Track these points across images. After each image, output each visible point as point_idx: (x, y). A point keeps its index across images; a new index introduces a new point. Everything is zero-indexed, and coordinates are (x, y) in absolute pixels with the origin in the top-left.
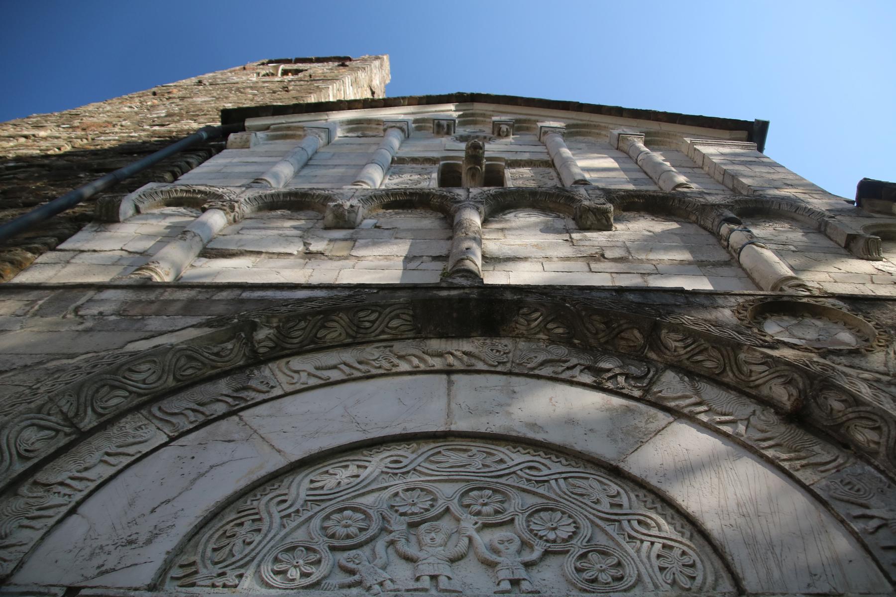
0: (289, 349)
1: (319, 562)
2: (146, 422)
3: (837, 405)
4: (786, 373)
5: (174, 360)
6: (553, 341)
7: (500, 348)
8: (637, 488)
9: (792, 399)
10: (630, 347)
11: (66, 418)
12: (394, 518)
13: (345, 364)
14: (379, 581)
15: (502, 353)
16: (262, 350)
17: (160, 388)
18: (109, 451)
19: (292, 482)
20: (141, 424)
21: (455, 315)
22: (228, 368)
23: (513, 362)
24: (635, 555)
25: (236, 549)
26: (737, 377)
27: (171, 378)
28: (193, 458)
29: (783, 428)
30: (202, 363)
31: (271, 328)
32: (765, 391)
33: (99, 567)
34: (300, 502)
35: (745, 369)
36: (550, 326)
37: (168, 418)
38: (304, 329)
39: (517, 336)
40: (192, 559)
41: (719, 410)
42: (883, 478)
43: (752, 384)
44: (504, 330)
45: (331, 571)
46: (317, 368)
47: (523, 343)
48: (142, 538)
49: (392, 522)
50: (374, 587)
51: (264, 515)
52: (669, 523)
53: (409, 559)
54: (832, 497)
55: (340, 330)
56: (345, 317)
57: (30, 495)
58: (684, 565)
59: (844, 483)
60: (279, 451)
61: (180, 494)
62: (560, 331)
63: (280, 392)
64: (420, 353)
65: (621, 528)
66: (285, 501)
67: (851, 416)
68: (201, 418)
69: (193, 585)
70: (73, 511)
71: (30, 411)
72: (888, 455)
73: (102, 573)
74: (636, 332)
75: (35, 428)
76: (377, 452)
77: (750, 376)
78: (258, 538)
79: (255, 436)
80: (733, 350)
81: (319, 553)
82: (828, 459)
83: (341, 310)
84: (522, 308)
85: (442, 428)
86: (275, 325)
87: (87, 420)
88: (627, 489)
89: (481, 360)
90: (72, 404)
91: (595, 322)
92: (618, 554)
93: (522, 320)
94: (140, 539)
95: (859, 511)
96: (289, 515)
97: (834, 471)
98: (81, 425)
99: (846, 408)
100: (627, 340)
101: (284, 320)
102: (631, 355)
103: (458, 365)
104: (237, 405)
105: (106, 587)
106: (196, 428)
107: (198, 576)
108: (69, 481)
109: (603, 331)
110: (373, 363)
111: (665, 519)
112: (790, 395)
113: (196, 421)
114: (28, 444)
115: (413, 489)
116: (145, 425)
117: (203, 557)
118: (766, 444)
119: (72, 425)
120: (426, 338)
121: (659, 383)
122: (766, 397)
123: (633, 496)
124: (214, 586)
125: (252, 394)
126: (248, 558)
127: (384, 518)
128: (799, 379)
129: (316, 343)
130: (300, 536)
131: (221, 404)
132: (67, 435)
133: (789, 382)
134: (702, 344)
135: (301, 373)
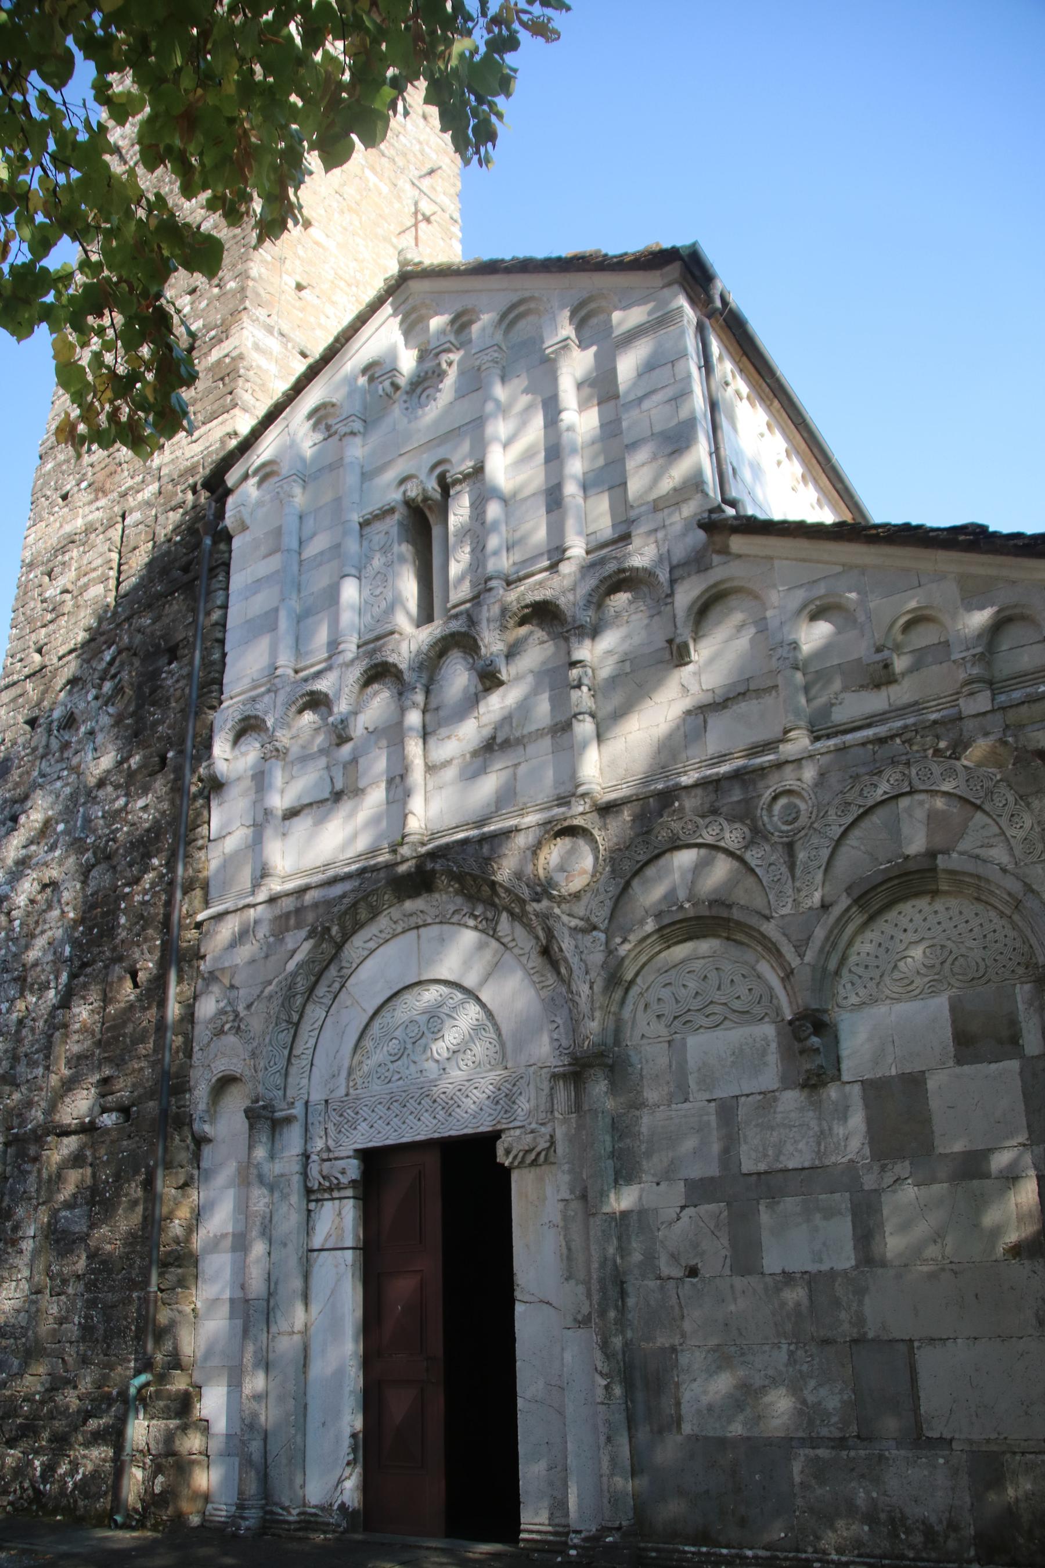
7: (435, 903)
11: (287, 1022)
16: (339, 940)
70: (312, 1065)
103: (421, 923)
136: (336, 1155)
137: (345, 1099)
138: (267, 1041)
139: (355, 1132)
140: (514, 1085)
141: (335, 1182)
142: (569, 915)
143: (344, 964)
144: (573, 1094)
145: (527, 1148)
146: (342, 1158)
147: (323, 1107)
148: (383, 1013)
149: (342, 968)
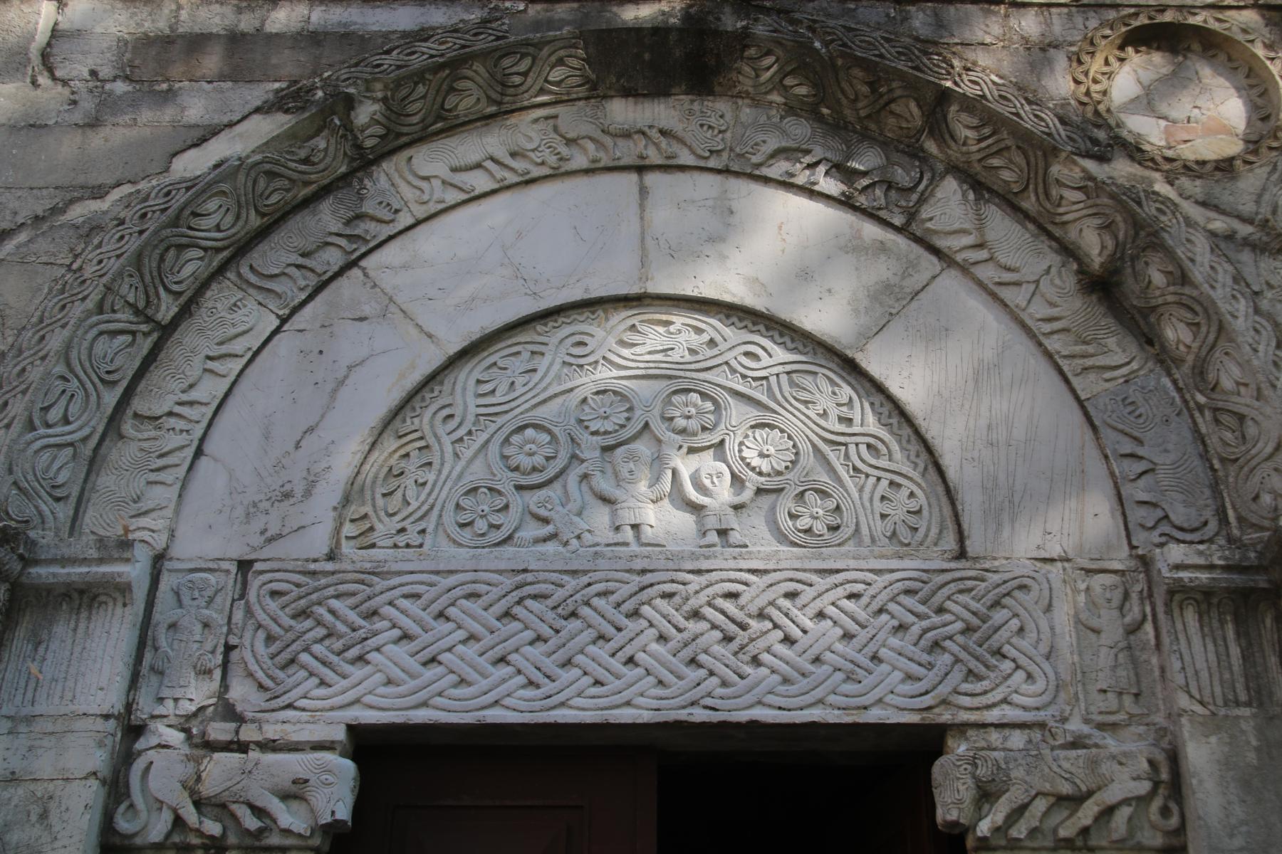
0: (407, 134)
1: (506, 507)
2: (240, 295)
3: (1158, 279)
4: (1107, 212)
5: (250, 184)
6: (791, 109)
7: (713, 121)
8: (873, 390)
9: (1106, 253)
10: (901, 128)
11: (137, 312)
12: (585, 438)
13: (493, 159)
14: (576, 534)
15: (716, 131)
16: (369, 143)
17: (243, 233)
18: (211, 354)
19: (454, 383)
20: (235, 299)
21: (647, 56)
22: (326, 182)
23: (731, 150)
24: (856, 495)
25: (411, 494)
26: (1040, 204)
27: (253, 212)
28: (321, 352)
29: (1078, 303)
30: (290, 179)
31: (375, 100)
32: (1072, 234)
33: (262, 533)
34: (470, 418)
35: (1054, 192)
36: (789, 81)
37: (269, 285)
38: (424, 97)
39: (739, 96)
40: (363, 510)
41: (1003, 261)
42: (1178, 400)
43: (1058, 219)
44: (720, 84)
45: (521, 520)
46: (455, 170)
47: (748, 110)
48: (299, 490)
49: (583, 446)
50: (571, 541)
51: (431, 440)
52: (902, 449)
53: (606, 500)
54: (1105, 422)
55: (477, 93)
56: (482, 70)
58: (908, 512)
59: (1127, 402)
60: (430, 336)
61: (323, 416)
62: (803, 90)
63: (410, 221)
64: (597, 134)
65: (847, 456)
66: (451, 416)
67: (1170, 298)
68: (313, 281)
69: (373, 546)
70: (199, 453)
71: (89, 314)
72: (1194, 367)
73: (270, 540)
74: (913, 105)
75: (106, 336)
76: (554, 327)
77: (1059, 205)
78: (431, 477)
79: (392, 308)
80: (1045, 155)
81: (505, 496)
82: (1122, 362)
83: (472, 57)
84: (746, 47)
85: (635, 289)
86: (380, 95)
87: (163, 307)
88: (862, 392)
89: (685, 144)
90: (136, 288)
91: (855, 81)
92: (837, 493)
93: (747, 69)
94: (296, 490)
95: (1128, 447)
96: (461, 440)
97: (1122, 380)
98: (159, 317)
99: (1168, 286)
100: (898, 116)
101: (392, 86)
102: (902, 142)
103: (654, 157)
104: (355, 250)
105: (280, 559)
106: (310, 298)
107: (376, 534)
108: (178, 409)
109: (866, 97)
110: (531, 154)
111: (899, 442)
112: (1103, 247)
113: (307, 286)
114: (106, 363)
115: (604, 392)
116: (240, 300)
117: (374, 506)
118: (1047, 328)
119: (149, 320)
120: (605, 97)
121: (932, 201)
122: (1073, 243)
123: (867, 405)
124: (396, 546)
125: (372, 226)
126: (425, 508)
127: (572, 440)
128: (1122, 225)
129: (445, 119)
130: (477, 473)
131: (332, 249)
132: (146, 335)
133: (1108, 227)
134: (1004, 139)
135: (432, 180)
136: (271, 732)
137: (329, 566)
138: (55, 342)
139: (357, 672)
140: (996, 604)
141: (251, 823)
142: (1204, 204)
143: (369, 207)
144: (1235, 651)
145: (1066, 789)
146: (294, 748)
147: (229, 582)
148: (495, 355)
149: (360, 217)
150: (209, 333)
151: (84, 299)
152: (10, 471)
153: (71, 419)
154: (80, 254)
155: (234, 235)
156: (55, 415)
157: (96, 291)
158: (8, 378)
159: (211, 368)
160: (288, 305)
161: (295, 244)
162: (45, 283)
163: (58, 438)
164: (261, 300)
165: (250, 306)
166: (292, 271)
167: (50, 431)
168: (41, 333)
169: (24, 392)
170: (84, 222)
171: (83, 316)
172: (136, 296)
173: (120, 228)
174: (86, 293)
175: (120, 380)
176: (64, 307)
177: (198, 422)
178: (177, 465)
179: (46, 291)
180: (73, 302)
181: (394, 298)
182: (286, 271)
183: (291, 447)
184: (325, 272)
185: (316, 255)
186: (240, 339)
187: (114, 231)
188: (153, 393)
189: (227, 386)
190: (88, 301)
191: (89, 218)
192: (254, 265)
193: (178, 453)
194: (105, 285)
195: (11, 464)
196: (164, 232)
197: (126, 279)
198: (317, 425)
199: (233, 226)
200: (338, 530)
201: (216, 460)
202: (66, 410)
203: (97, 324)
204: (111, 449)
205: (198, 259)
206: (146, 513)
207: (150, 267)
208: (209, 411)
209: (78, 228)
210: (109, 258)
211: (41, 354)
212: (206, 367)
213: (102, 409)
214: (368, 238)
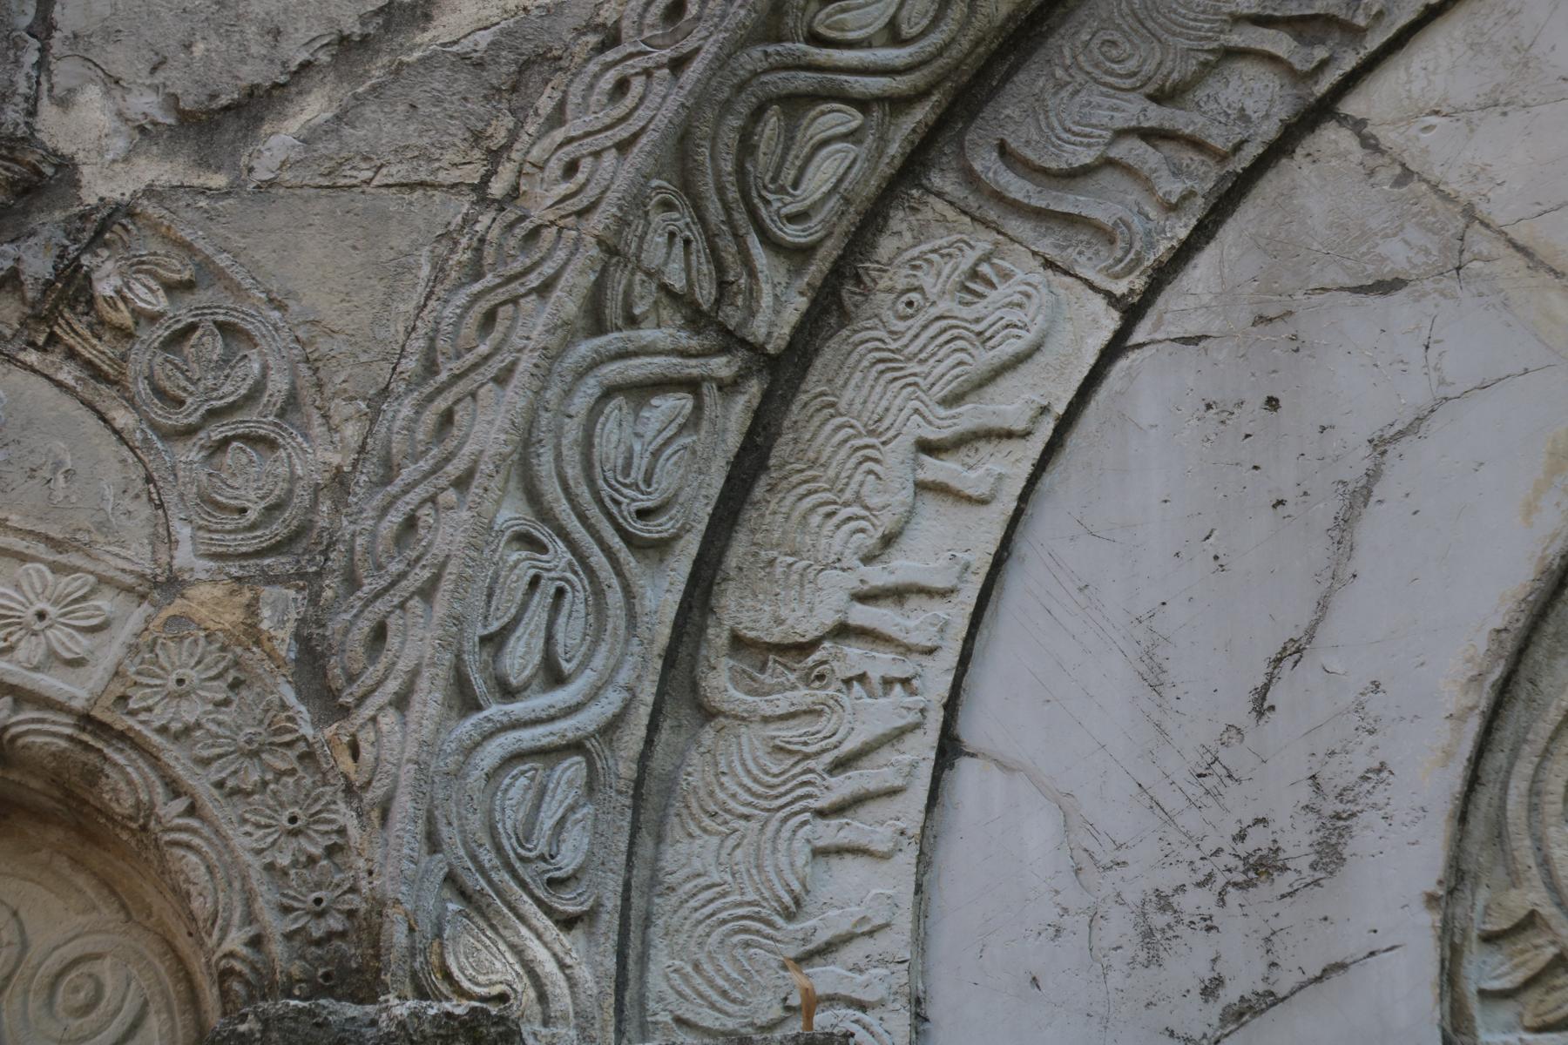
2: (984, 241)
11: (697, 319)
17: (965, 44)
18: (932, 434)
20: (971, 257)
28: (1272, 403)
33: (1210, 990)
37: (1068, 202)
48: (1298, 841)
57: (764, 707)
61: (1323, 606)
68: (1205, 178)
70: (949, 749)
71: (568, 334)
75: (619, 400)
79: (1480, 241)
87: (766, 300)
90: (687, 242)
94: (1289, 850)
98: (758, 329)
104: (1323, 65)
106: (1203, 233)
108: (862, 615)
113: (1189, 195)
116: (986, 258)
119: (731, 340)
131: (1248, 70)
132: (728, 388)
150: (914, 367)
151: (545, 289)
152: (433, 843)
153: (567, 667)
154: (507, 147)
155: (940, 52)
156: (521, 658)
157: (579, 261)
158: (369, 551)
159: (941, 477)
160: (1138, 261)
161: (1132, 65)
162: (416, 246)
163: (540, 730)
164: (1052, 254)
165: (1020, 275)
166: (1133, 151)
167: (518, 708)
168: (441, 404)
169: (427, 592)
170: (493, 44)
171: (554, 341)
172: (688, 269)
173: (611, 55)
174: (548, 269)
175: (676, 537)
176: (490, 318)
177: (930, 651)
178: (892, 792)
179: (425, 271)
180: (514, 301)
181: (1482, 208)
182: (1114, 153)
183: (1241, 713)
184: (1238, 148)
185: (1201, 94)
186: (1007, 382)
187: (593, 67)
188: (779, 570)
189: (998, 533)
190: (557, 293)
191: (508, 33)
192: (1013, 144)
193: (886, 754)
194: (600, 242)
195: (431, 820)
196: (744, 58)
197: (657, 218)
198: (1311, 634)
199: (935, 22)
200: (1450, 975)
201: (1004, 767)
202: (549, 639)
203: (594, 365)
204: (683, 754)
205: (844, 137)
206: (828, 949)
207: (718, 174)
208: (958, 612)
209: (480, 65)
210: (597, 154)
211: (454, 469)
212: (922, 475)
213: (642, 630)
214: (1361, 21)
